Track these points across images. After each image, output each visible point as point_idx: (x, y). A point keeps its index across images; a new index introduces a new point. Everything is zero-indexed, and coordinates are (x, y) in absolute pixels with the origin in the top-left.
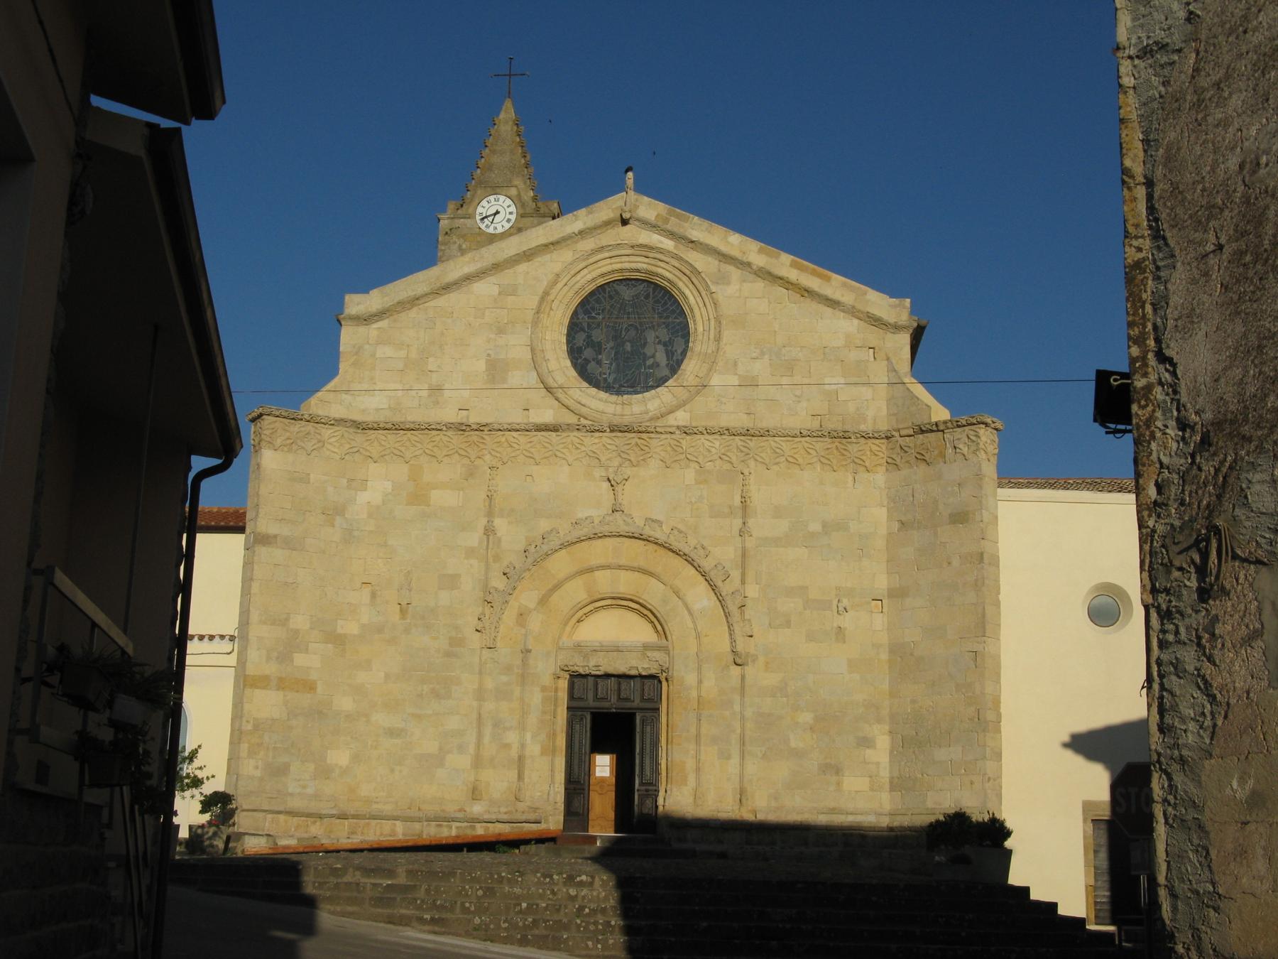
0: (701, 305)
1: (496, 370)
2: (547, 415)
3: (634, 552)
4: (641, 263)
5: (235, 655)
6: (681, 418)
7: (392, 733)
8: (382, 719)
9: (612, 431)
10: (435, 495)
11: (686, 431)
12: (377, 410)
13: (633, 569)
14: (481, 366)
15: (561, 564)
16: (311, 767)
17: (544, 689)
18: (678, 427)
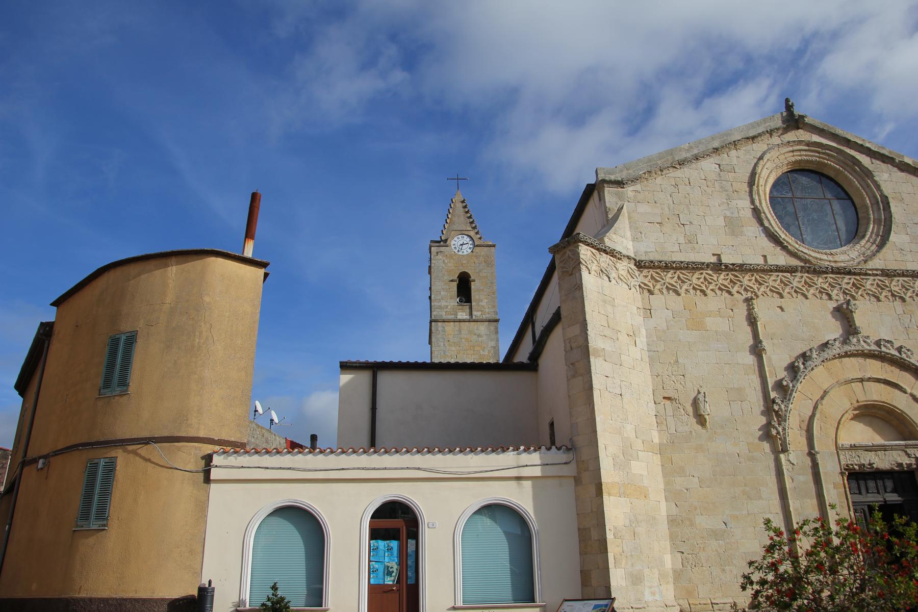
0: (865, 187)
1: (732, 226)
2: (780, 258)
3: (876, 369)
4: (814, 157)
5: (573, 465)
6: (877, 263)
7: (715, 534)
8: (704, 522)
9: (832, 272)
10: (709, 321)
11: (887, 274)
12: (646, 252)
13: (878, 381)
14: (721, 222)
15: (818, 377)
16: (656, 571)
17: (835, 486)
18: (882, 270)
